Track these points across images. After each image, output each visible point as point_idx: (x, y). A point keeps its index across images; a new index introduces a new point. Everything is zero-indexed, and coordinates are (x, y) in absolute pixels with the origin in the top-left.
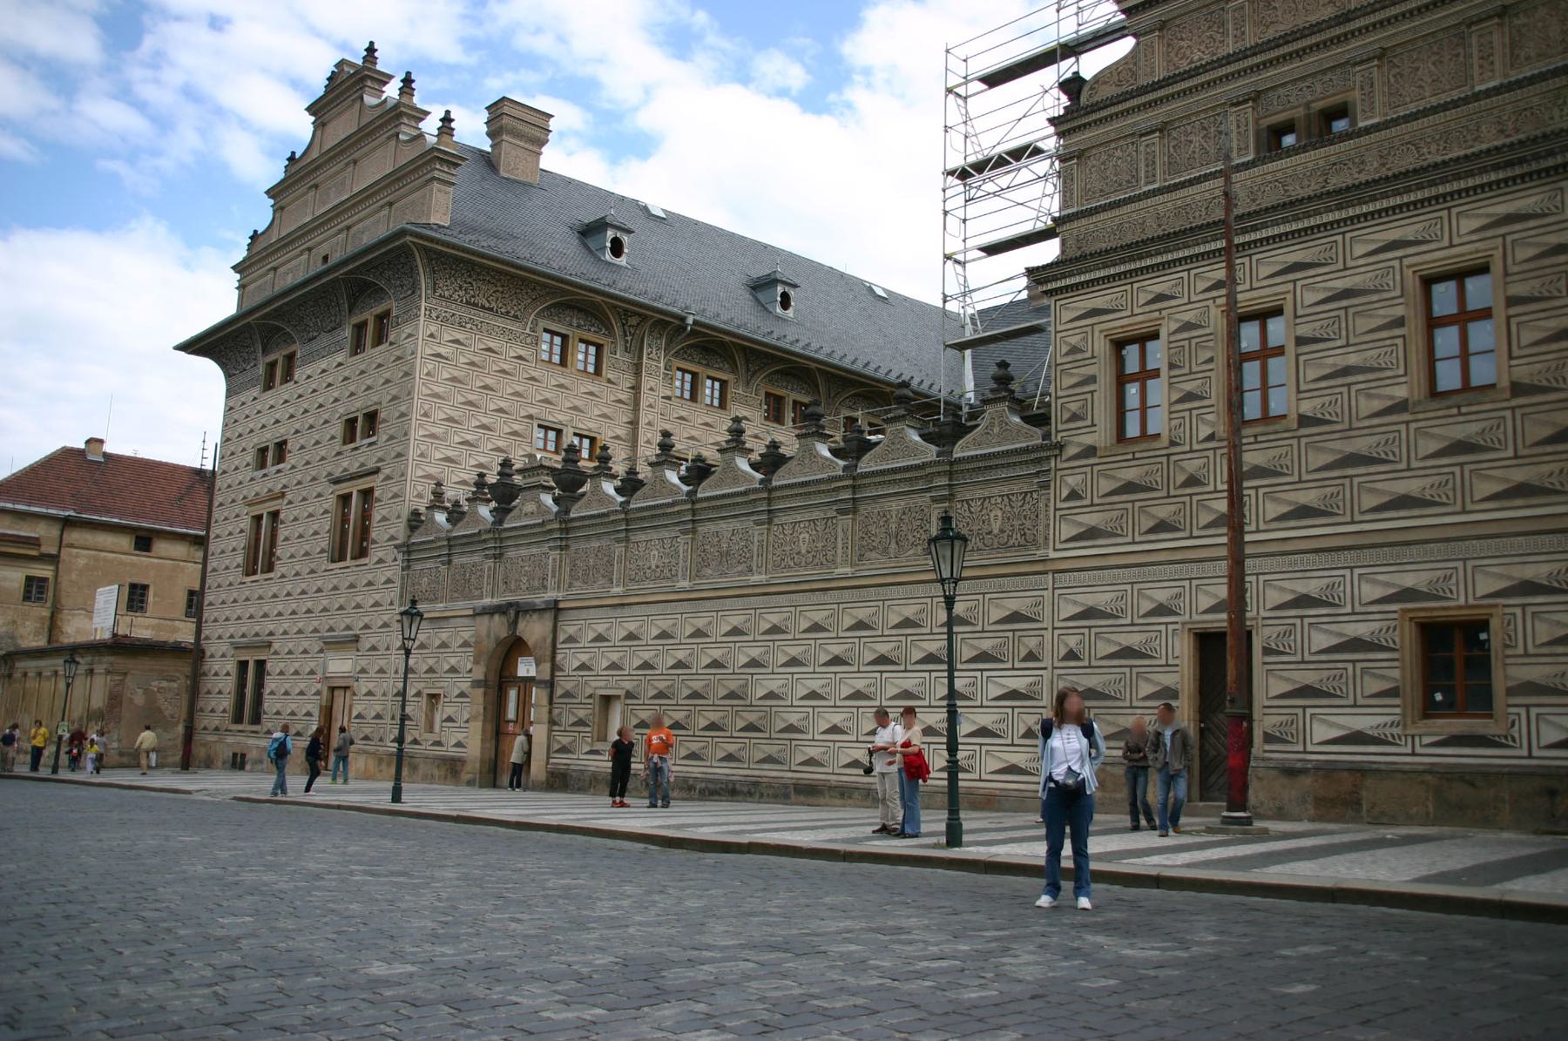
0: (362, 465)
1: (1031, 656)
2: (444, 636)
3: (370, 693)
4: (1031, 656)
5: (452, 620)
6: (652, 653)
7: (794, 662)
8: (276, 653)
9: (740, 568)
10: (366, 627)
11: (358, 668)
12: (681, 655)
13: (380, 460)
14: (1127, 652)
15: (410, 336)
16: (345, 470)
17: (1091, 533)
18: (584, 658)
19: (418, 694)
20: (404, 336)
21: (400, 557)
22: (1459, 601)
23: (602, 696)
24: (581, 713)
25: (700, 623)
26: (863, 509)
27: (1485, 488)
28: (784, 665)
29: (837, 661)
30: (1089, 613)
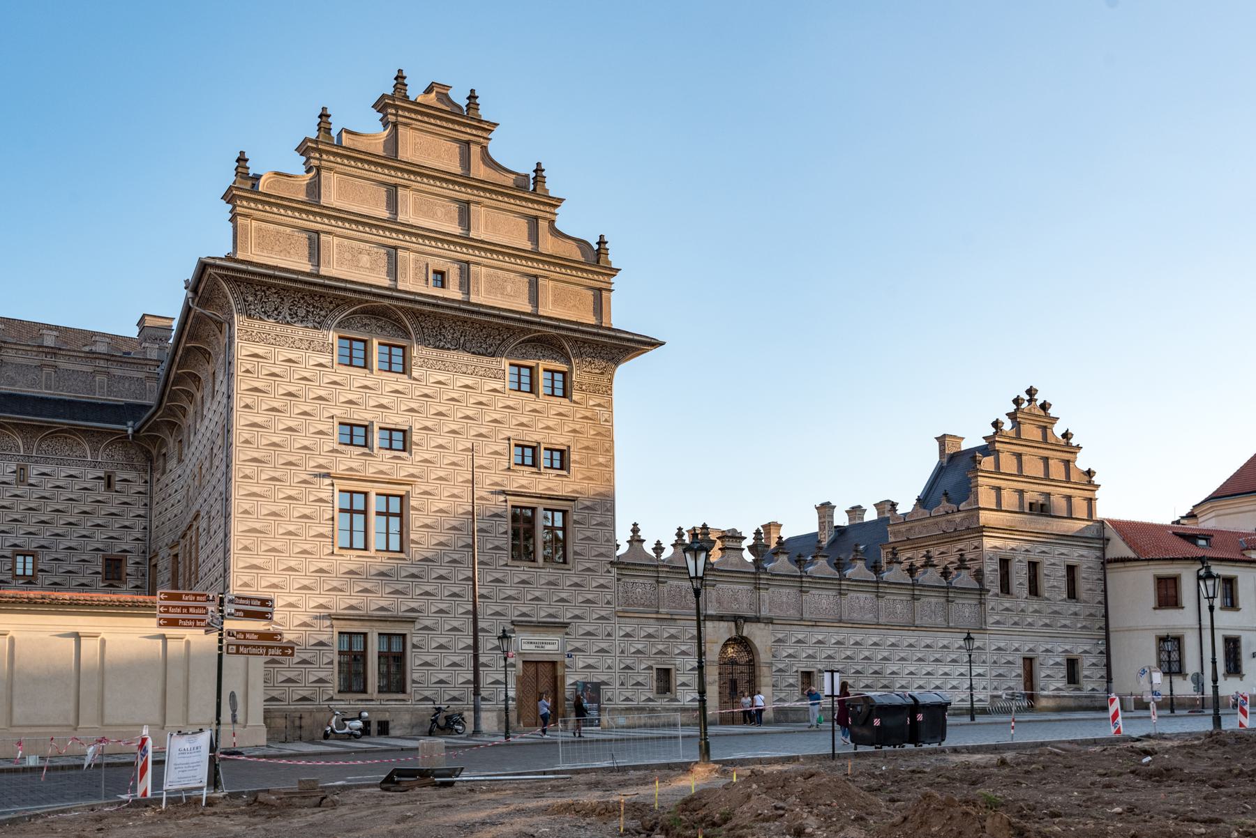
0: (549, 489)
1: (984, 662)
2: (673, 631)
3: (589, 666)
4: (984, 662)
5: (678, 621)
6: (832, 652)
7: (902, 659)
8: (426, 628)
9: (871, 615)
10: (576, 617)
11: (569, 648)
12: (849, 653)
13: (578, 492)
14: (1009, 662)
15: (599, 405)
16: (522, 486)
17: (998, 623)
18: (791, 651)
19: (650, 668)
20: (591, 403)
21: (614, 571)
22: (1074, 655)
23: (802, 672)
24: (791, 681)
25: (858, 639)
26: (923, 599)
27: (1079, 625)
28: (899, 660)
29: (920, 660)
30: (999, 649)
